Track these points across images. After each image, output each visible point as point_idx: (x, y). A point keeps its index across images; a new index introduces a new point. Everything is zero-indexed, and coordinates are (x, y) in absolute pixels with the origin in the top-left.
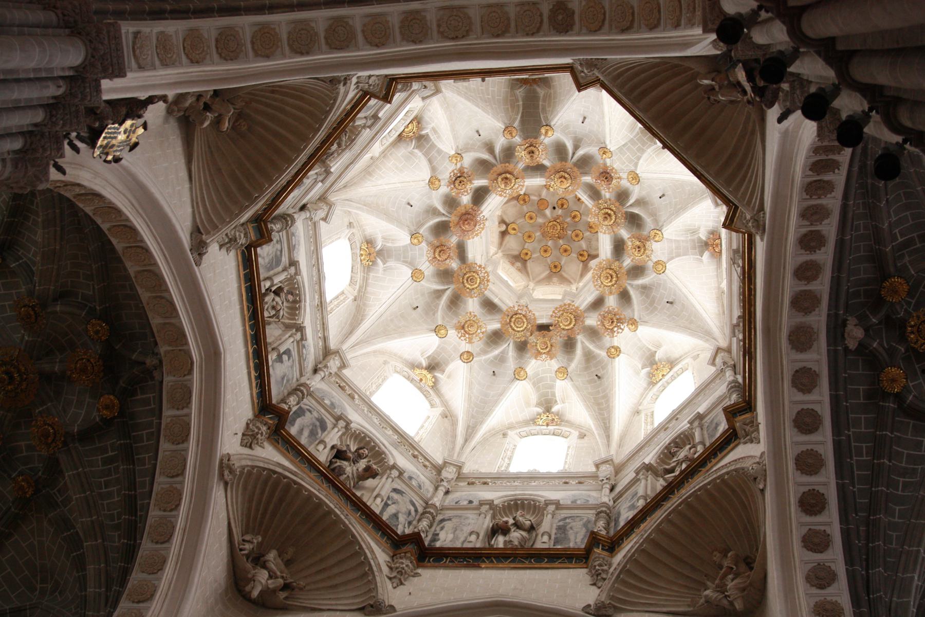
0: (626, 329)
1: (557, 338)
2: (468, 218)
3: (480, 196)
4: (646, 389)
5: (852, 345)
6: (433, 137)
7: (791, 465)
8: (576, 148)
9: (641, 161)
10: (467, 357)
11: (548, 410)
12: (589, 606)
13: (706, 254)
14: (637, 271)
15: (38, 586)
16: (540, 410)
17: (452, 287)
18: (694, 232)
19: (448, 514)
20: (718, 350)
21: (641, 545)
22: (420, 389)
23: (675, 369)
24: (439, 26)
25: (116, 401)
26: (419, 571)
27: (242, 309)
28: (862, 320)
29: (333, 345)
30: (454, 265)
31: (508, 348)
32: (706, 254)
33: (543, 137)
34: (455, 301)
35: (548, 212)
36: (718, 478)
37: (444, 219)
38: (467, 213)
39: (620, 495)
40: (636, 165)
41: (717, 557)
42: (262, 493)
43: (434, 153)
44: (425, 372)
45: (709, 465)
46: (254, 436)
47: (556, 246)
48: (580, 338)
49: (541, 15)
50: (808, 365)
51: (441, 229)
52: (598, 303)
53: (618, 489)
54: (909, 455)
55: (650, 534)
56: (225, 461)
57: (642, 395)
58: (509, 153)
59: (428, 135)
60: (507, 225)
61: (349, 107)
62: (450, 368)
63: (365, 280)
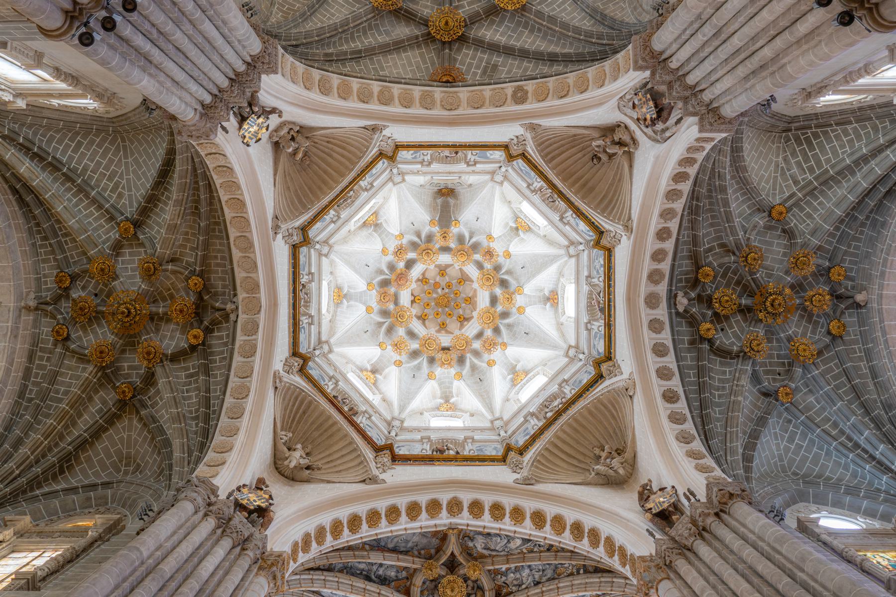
0: (499, 349)
1: (454, 355)
2: (402, 277)
3: (410, 264)
4: (510, 389)
5: (681, 309)
6: (384, 225)
7: (654, 375)
8: (471, 237)
9: (511, 246)
10: (398, 364)
11: (447, 401)
12: (517, 479)
13: (548, 304)
14: (505, 315)
15: (123, 469)
16: (442, 401)
17: (389, 320)
18: (541, 290)
19: (401, 444)
20: (570, 347)
21: (545, 445)
22: (366, 384)
23: (529, 376)
24: (441, 101)
25: (202, 334)
26: (394, 466)
27: (289, 284)
28: (686, 294)
29: (324, 339)
30: (391, 307)
31: (423, 360)
32: (548, 304)
33: (452, 228)
34: (390, 330)
35: (439, 290)
36: (595, 399)
37: (387, 277)
38: (401, 274)
39: (514, 433)
40: (508, 248)
41: (597, 451)
42: (293, 405)
43: (383, 236)
44: (369, 374)
45: (585, 396)
46: (291, 367)
47: (443, 311)
48: (468, 355)
49: (506, 95)
50: (658, 317)
51: (385, 283)
52: (479, 335)
53: (509, 432)
54: (719, 379)
55: (550, 439)
56: (277, 373)
57: (508, 392)
58: (430, 238)
59: (381, 224)
60: (415, 297)
61: (371, 160)
62: (387, 371)
63: (335, 312)
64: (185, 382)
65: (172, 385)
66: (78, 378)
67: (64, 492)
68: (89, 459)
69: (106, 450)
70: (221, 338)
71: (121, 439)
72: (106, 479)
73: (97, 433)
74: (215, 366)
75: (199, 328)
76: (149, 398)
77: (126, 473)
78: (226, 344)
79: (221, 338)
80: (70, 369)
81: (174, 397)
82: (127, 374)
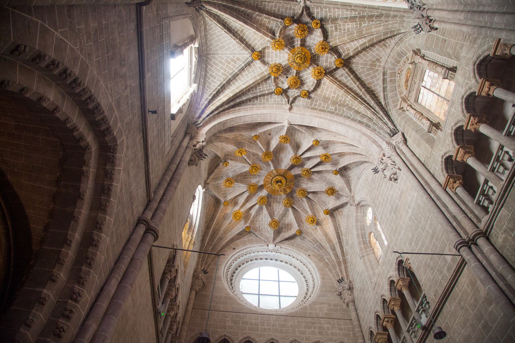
15: (377, 68)
64: (339, 32)
65: (340, 37)
66: (328, 87)
67: (385, 92)
68: (369, 83)
69: (366, 76)
70: (318, 12)
71: (362, 68)
72: (381, 75)
73: (358, 79)
74: (333, 15)
75: (312, 23)
76: (344, 52)
77: (379, 66)
78: (322, 9)
79: (318, 12)
80: (323, 91)
81: (347, 35)
82: (329, 64)
